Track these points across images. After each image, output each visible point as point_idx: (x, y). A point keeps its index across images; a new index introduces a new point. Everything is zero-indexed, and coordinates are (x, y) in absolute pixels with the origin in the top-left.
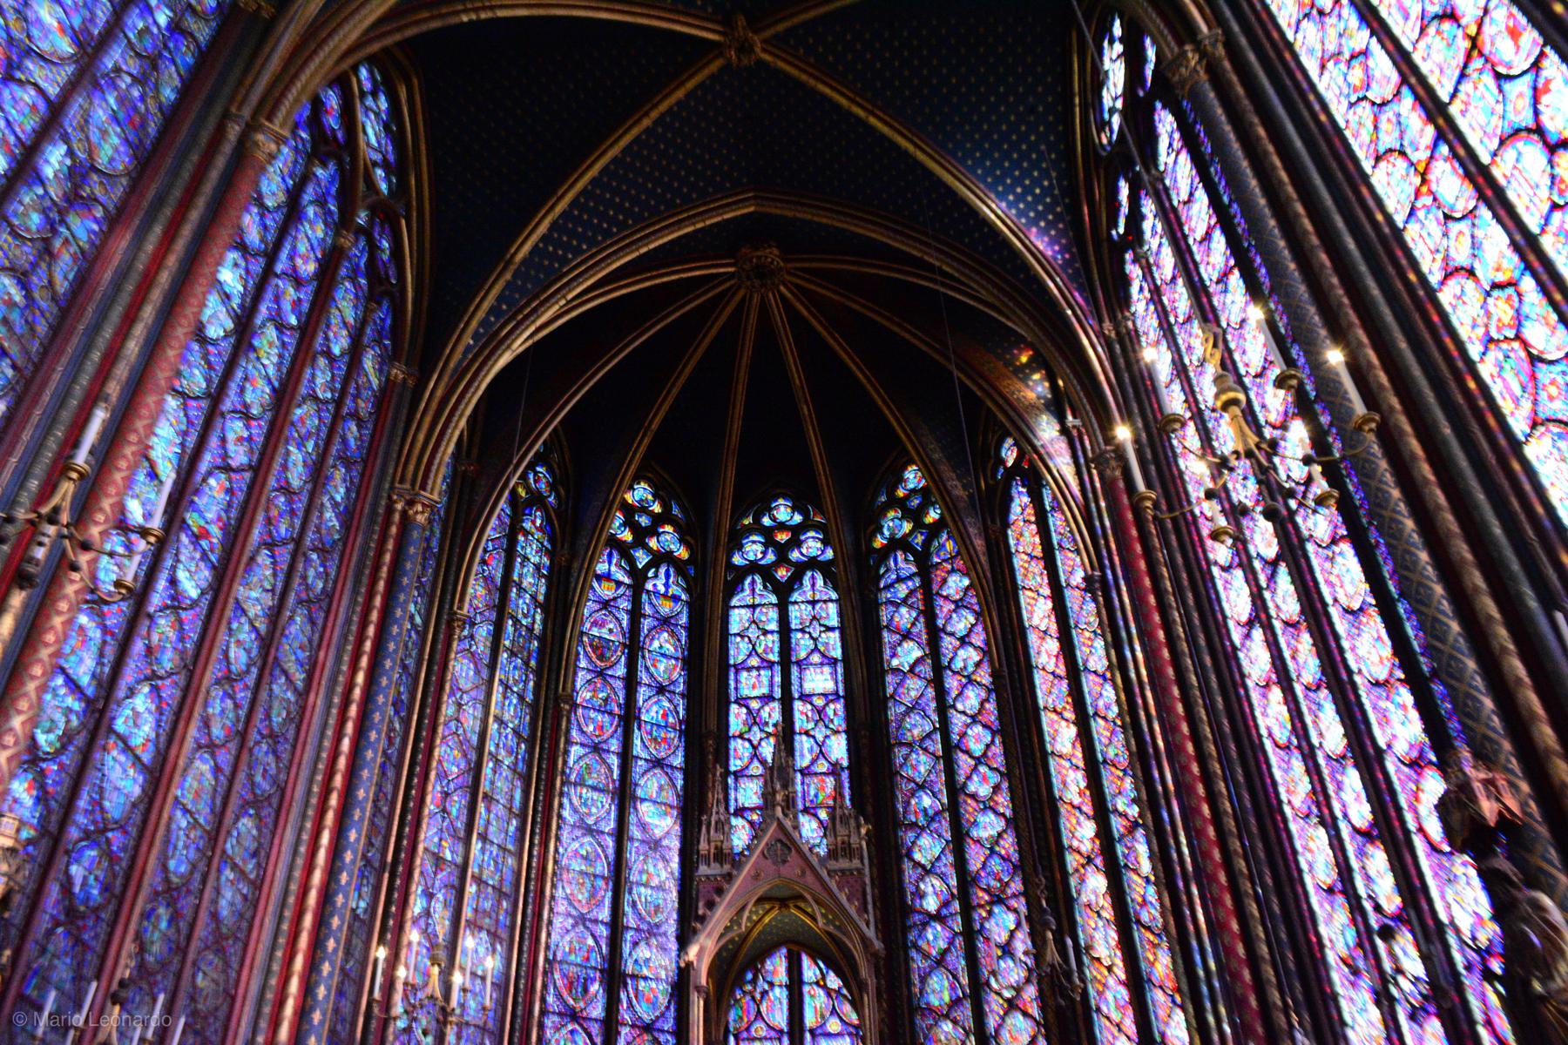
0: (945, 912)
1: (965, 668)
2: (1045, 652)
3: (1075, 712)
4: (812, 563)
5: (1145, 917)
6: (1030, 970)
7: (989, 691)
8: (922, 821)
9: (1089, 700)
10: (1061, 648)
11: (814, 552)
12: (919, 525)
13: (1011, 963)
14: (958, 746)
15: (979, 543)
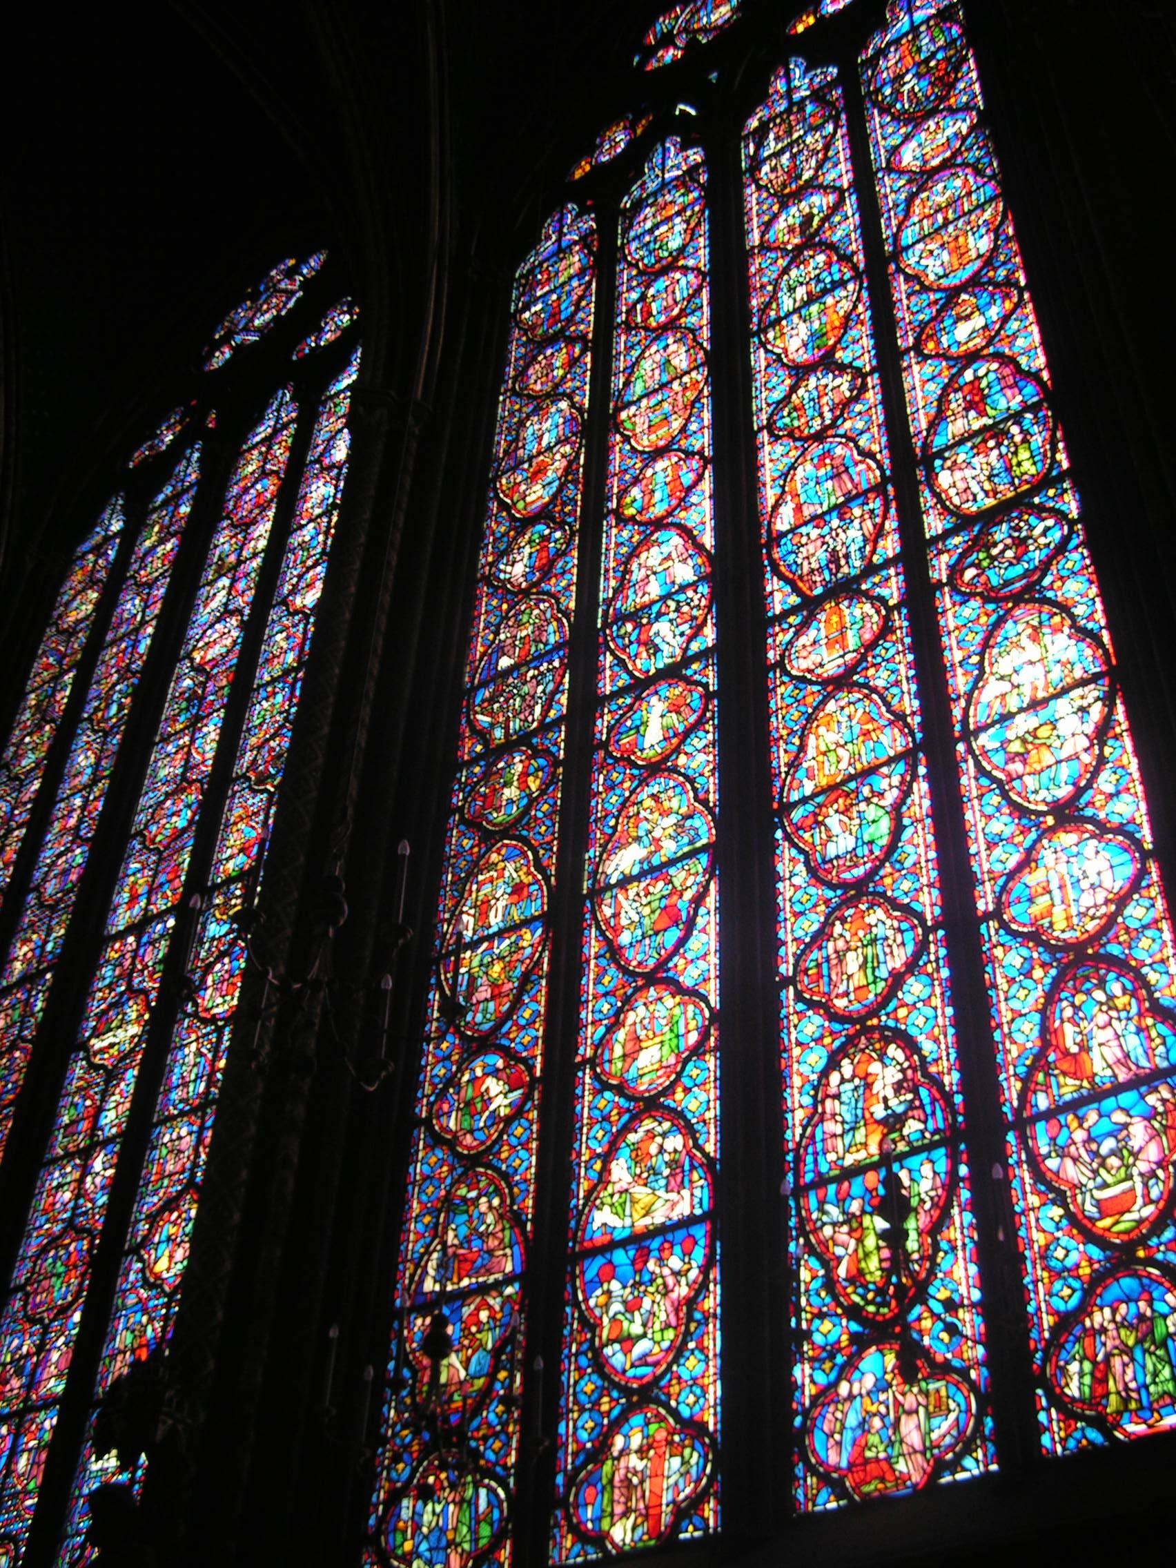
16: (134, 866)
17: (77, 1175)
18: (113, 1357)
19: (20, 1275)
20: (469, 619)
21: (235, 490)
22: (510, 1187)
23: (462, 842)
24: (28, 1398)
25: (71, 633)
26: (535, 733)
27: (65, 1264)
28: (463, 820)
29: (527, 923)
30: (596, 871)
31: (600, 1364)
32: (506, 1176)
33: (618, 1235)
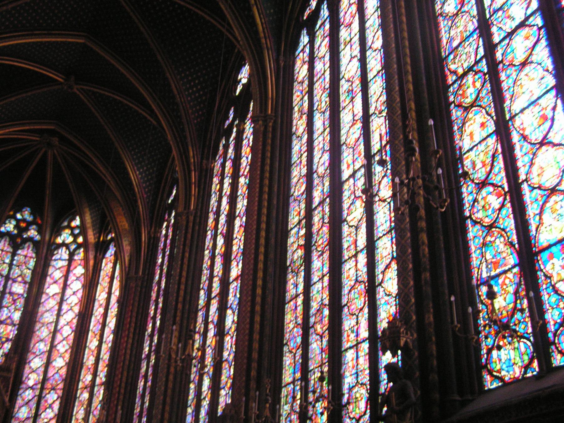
0: (35, 387)
1: (71, 303)
2: (98, 311)
3: (100, 337)
4: (30, 239)
5: (95, 413)
6: (56, 415)
7: (76, 316)
8: (38, 353)
9: (105, 336)
10: (104, 313)
11: (32, 235)
12: (75, 241)
13: (51, 410)
14: (59, 331)
15: (92, 262)
16: (345, 154)
17: (354, 263)
18: (381, 321)
19: (344, 301)
20: (438, 32)
21: (342, 15)
22: (506, 233)
23: (456, 113)
24: (357, 340)
25: (302, 82)
26: (473, 66)
27: (358, 294)
28: (455, 106)
29: (488, 136)
30: (510, 111)
31: (556, 291)
32: (503, 230)
33: (552, 242)
